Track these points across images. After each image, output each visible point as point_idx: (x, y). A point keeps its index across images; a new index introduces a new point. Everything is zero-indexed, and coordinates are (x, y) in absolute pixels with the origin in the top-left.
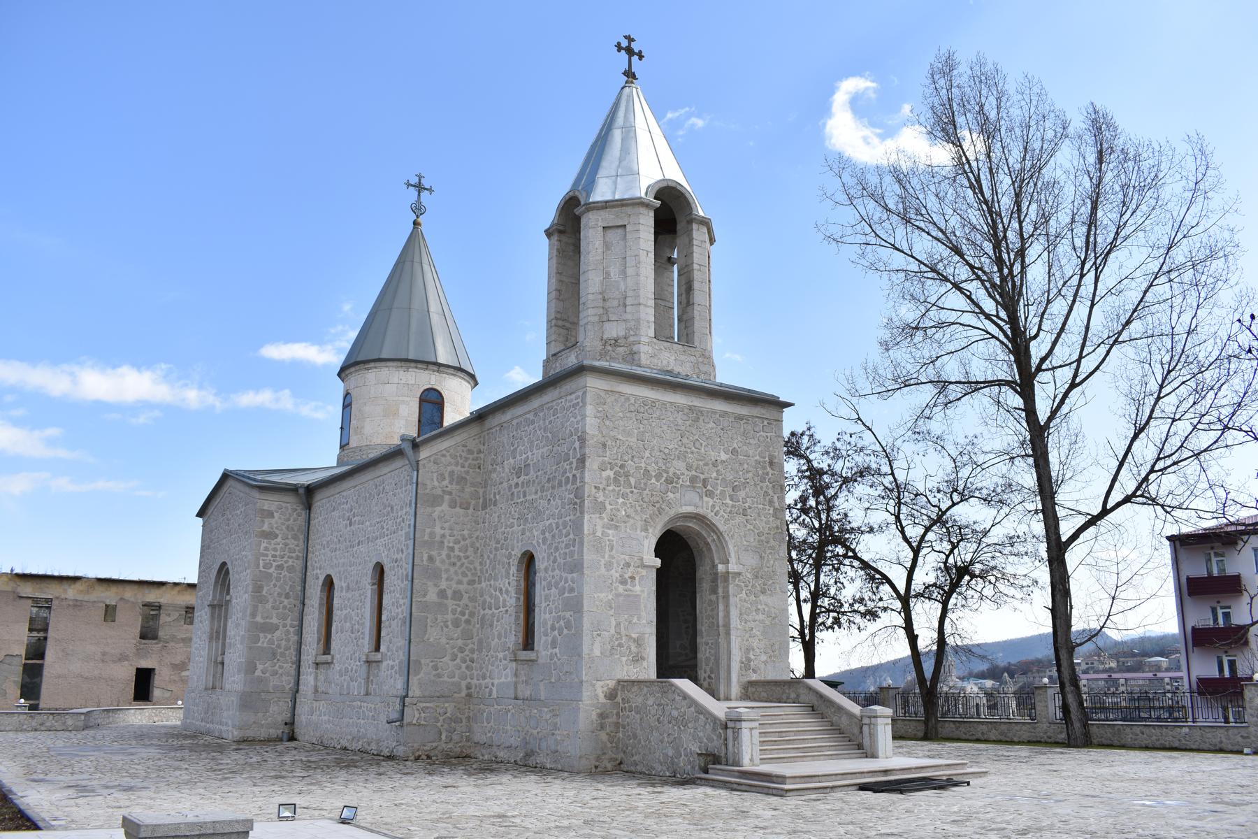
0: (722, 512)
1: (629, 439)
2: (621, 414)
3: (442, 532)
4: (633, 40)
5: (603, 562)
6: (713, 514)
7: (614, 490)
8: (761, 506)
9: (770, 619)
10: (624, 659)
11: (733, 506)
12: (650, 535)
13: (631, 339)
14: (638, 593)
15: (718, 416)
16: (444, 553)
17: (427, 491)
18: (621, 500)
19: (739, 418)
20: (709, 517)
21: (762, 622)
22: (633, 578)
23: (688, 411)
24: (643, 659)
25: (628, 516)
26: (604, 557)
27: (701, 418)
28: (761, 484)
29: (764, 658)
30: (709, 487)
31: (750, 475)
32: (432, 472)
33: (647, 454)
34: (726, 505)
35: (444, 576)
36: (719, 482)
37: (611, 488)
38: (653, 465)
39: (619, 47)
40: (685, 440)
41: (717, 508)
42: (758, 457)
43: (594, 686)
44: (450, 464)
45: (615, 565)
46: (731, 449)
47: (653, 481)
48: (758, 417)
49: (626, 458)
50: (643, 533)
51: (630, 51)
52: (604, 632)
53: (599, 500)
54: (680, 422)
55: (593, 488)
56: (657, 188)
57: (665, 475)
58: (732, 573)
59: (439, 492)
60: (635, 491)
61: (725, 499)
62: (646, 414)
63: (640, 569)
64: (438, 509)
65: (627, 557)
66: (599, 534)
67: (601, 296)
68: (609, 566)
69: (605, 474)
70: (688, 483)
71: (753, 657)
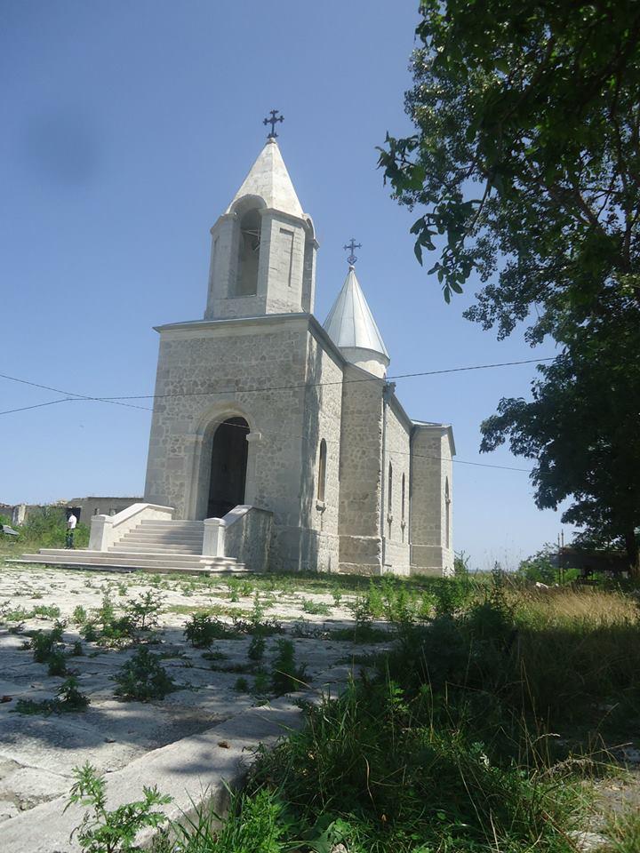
4: (277, 112)
21: (276, 470)
22: (179, 448)
31: (276, 371)
39: (266, 122)
41: (246, 397)
42: (282, 359)
54: (222, 347)
66: (160, 424)
68: (165, 442)
69: (167, 389)
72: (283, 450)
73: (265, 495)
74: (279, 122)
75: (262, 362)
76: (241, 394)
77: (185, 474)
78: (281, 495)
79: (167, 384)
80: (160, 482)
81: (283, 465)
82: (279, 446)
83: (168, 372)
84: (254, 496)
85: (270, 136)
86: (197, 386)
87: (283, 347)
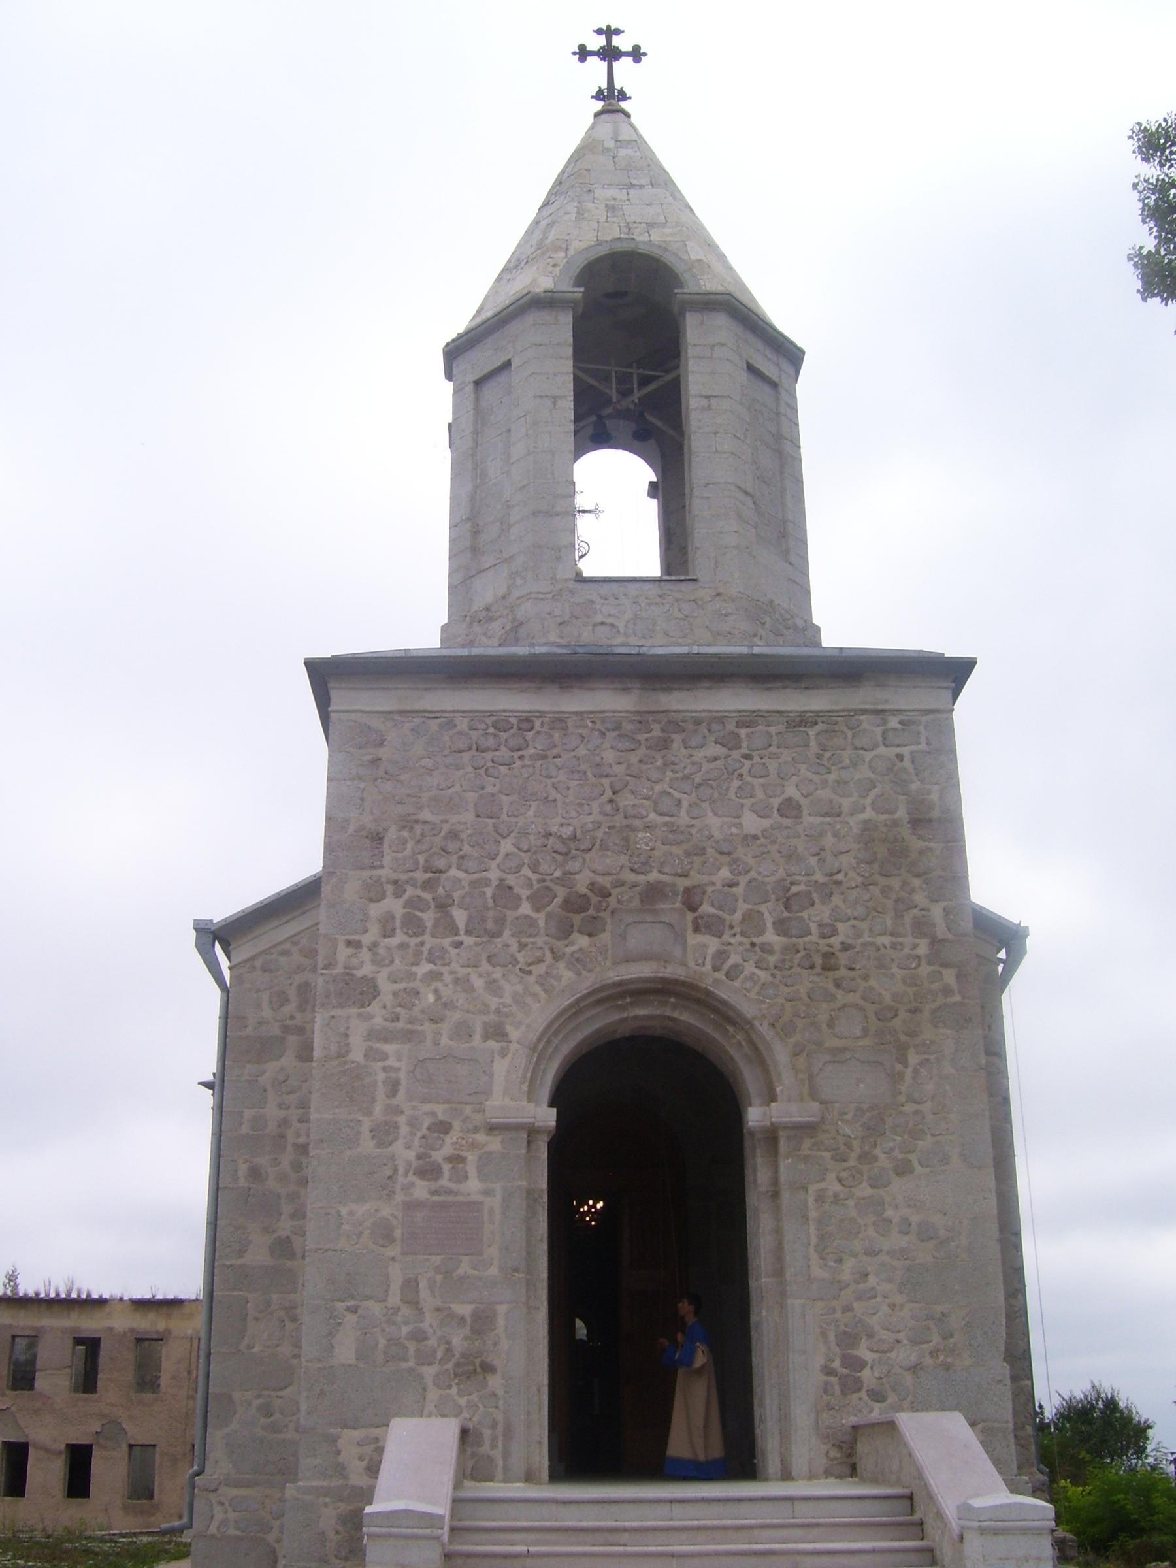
0: (749, 968)
1: (454, 819)
2: (427, 762)
3: (283, 1113)
4: (618, 32)
5: (367, 1124)
6: (721, 975)
7: (403, 946)
8: (886, 940)
9: (931, 1244)
10: (429, 1372)
11: (786, 949)
12: (514, 1046)
13: (516, 594)
14: (480, 1198)
15: (731, 726)
16: (286, 1160)
17: (249, 1031)
18: (424, 968)
19: (803, 721)
20: (708, 983)
22: (457, 1160)
23: (630, 727)
24: (488, 1368)
25: (445, 1005)
26: (369, 1113)
27: (677, 738)
28: (883, 881)
29: (905, 1355)
30: (706, 908)
31: (846, 861)
32: (258, 991)
33: (507, 846)
34: (767, 949)
35: (287, 1209)
36: (739, 891)
37: (394, 941)
38: (526, 871)
39: (583, 53)
40: (626, 800)
41: (734, 959)
42: (869, 814)
43: (334, 1440)
44: (300, 969)
45: (404, 1130)
46: (776, 802)
47: (526, 909)
48: (864, 712)
49: (441, 863)
50: (493, 1044)
51: (610, 54)
52: (371, 1303)
53: (359, 973)
54: (609, 756)
55: (341, 947)
56: (581, 262)
57: (561, 893)
58: (786, 1127)
59: (276, 1030)
60: (468, 940)
61: (762, 932)
62: (504, 753)
63: (481, 1137)
64: (271, 1068)
65: (441, 1111)
66: (357, 1055)
67: (468, 526)
68: (385, 1133)
69: (375, 910)
70: (636, 903)
71: (868, 1356)
72: (919, 1169)
73: (863, 1352)
74: (626, 61)
75: (786, 822)
76: (713, 944)
77: (493, 1271)
78: (933, 1354)
79: (374, 892)
80: (376, 1309)
81: (926, 1233)
82: (897, 1154)
83: (378, 838)
84: (820, 1361)
85: (599, 96)
86: (518, 907)
87: (864, 773)
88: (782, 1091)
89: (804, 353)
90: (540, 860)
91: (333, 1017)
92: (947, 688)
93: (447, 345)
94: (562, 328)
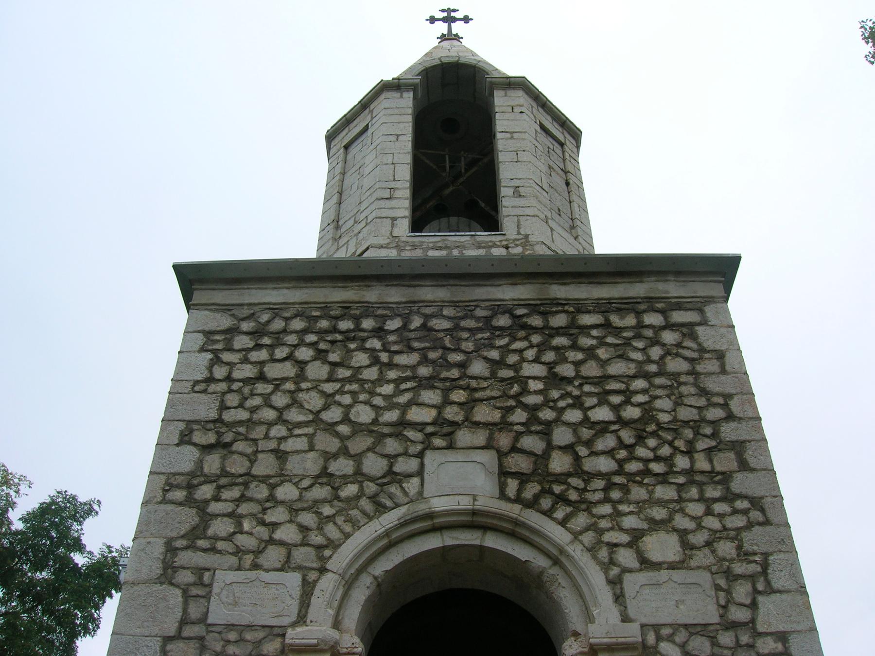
4: (455, 11)
39: (432, 20)
51: (449, 19)
88: (599, 614)
89: (581, 132)
90: (361, 412)
91: (149, 543)
92: (720, 282)
93: (328, 131)
94: (407, 101)
